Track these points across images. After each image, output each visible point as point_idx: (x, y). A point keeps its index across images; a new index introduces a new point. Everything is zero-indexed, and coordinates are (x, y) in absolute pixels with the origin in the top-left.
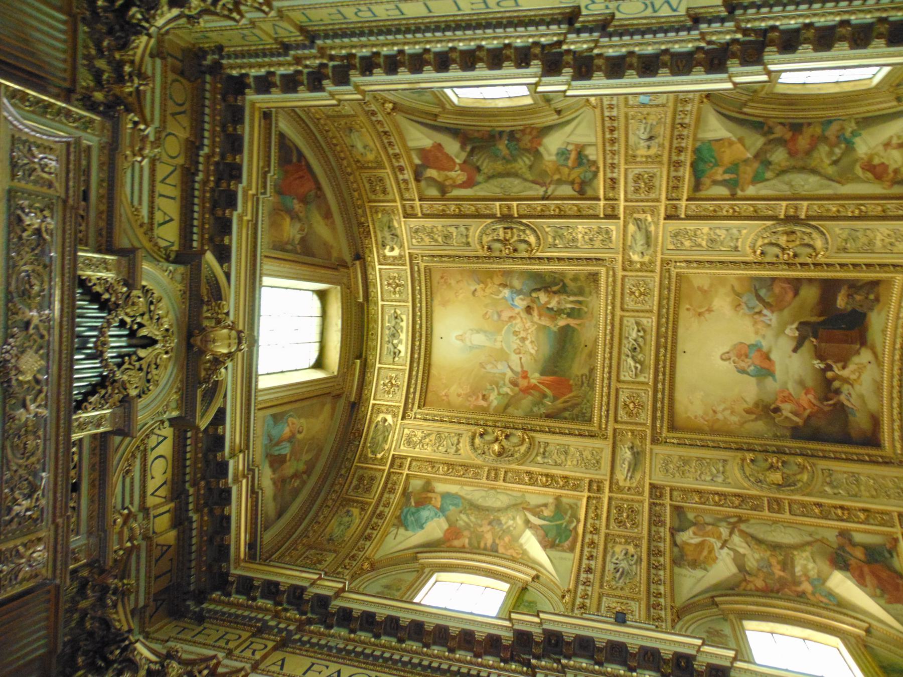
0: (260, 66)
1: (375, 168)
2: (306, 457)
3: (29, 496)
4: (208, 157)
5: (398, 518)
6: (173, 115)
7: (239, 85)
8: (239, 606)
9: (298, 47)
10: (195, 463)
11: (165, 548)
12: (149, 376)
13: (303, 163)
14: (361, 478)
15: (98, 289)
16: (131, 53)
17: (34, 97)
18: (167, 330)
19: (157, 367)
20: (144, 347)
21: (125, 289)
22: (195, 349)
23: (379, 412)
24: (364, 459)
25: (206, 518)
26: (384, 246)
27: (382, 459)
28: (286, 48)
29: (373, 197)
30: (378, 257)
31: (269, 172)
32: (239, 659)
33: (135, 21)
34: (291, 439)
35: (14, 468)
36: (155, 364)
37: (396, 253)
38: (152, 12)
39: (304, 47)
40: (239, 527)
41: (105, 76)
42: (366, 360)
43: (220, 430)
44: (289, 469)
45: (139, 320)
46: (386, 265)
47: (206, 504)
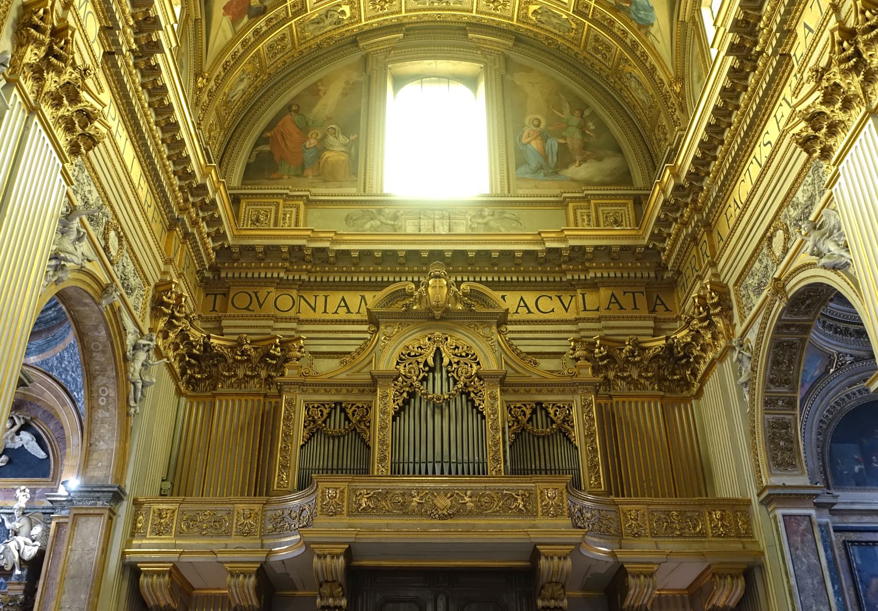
0: (204, 244)
1: (260, 58)
2: (566, 114)
3: (516, 499)
4: (287, 270)
5: (640, 27)
6: (261, 306)
7: (224, 252)
8: (673, 246)
10: (546, 272)
11: (613, 300)
12: (464, 354)
13: (269, 134)
14: (596, 50)
15: (400, 402)
17: (281, 444)
18: (429, 339)
19: (457, 347)
20: (442, 359)
22: (444, 315)
23: (526, 16)
24: (575, 41)
25: (594, 265)
26: (339, 21)
27: (577, 24)
28: (187, 235)
29: (289, 46)
30: (352, 24)
31: (287, 194)
32: (705, 272)
33: (202, 348)
34: (544, 137)
35: (498, 508)
36: (454, 349)
37: (346, 8)
38: (194, 343)
39: (184, 224)
41: (249, 373)
42: (469, 24)
43: (518, 255)
44: (574, 139)
45: (421, 366)
46: (360, 15)
47: (583, 264)
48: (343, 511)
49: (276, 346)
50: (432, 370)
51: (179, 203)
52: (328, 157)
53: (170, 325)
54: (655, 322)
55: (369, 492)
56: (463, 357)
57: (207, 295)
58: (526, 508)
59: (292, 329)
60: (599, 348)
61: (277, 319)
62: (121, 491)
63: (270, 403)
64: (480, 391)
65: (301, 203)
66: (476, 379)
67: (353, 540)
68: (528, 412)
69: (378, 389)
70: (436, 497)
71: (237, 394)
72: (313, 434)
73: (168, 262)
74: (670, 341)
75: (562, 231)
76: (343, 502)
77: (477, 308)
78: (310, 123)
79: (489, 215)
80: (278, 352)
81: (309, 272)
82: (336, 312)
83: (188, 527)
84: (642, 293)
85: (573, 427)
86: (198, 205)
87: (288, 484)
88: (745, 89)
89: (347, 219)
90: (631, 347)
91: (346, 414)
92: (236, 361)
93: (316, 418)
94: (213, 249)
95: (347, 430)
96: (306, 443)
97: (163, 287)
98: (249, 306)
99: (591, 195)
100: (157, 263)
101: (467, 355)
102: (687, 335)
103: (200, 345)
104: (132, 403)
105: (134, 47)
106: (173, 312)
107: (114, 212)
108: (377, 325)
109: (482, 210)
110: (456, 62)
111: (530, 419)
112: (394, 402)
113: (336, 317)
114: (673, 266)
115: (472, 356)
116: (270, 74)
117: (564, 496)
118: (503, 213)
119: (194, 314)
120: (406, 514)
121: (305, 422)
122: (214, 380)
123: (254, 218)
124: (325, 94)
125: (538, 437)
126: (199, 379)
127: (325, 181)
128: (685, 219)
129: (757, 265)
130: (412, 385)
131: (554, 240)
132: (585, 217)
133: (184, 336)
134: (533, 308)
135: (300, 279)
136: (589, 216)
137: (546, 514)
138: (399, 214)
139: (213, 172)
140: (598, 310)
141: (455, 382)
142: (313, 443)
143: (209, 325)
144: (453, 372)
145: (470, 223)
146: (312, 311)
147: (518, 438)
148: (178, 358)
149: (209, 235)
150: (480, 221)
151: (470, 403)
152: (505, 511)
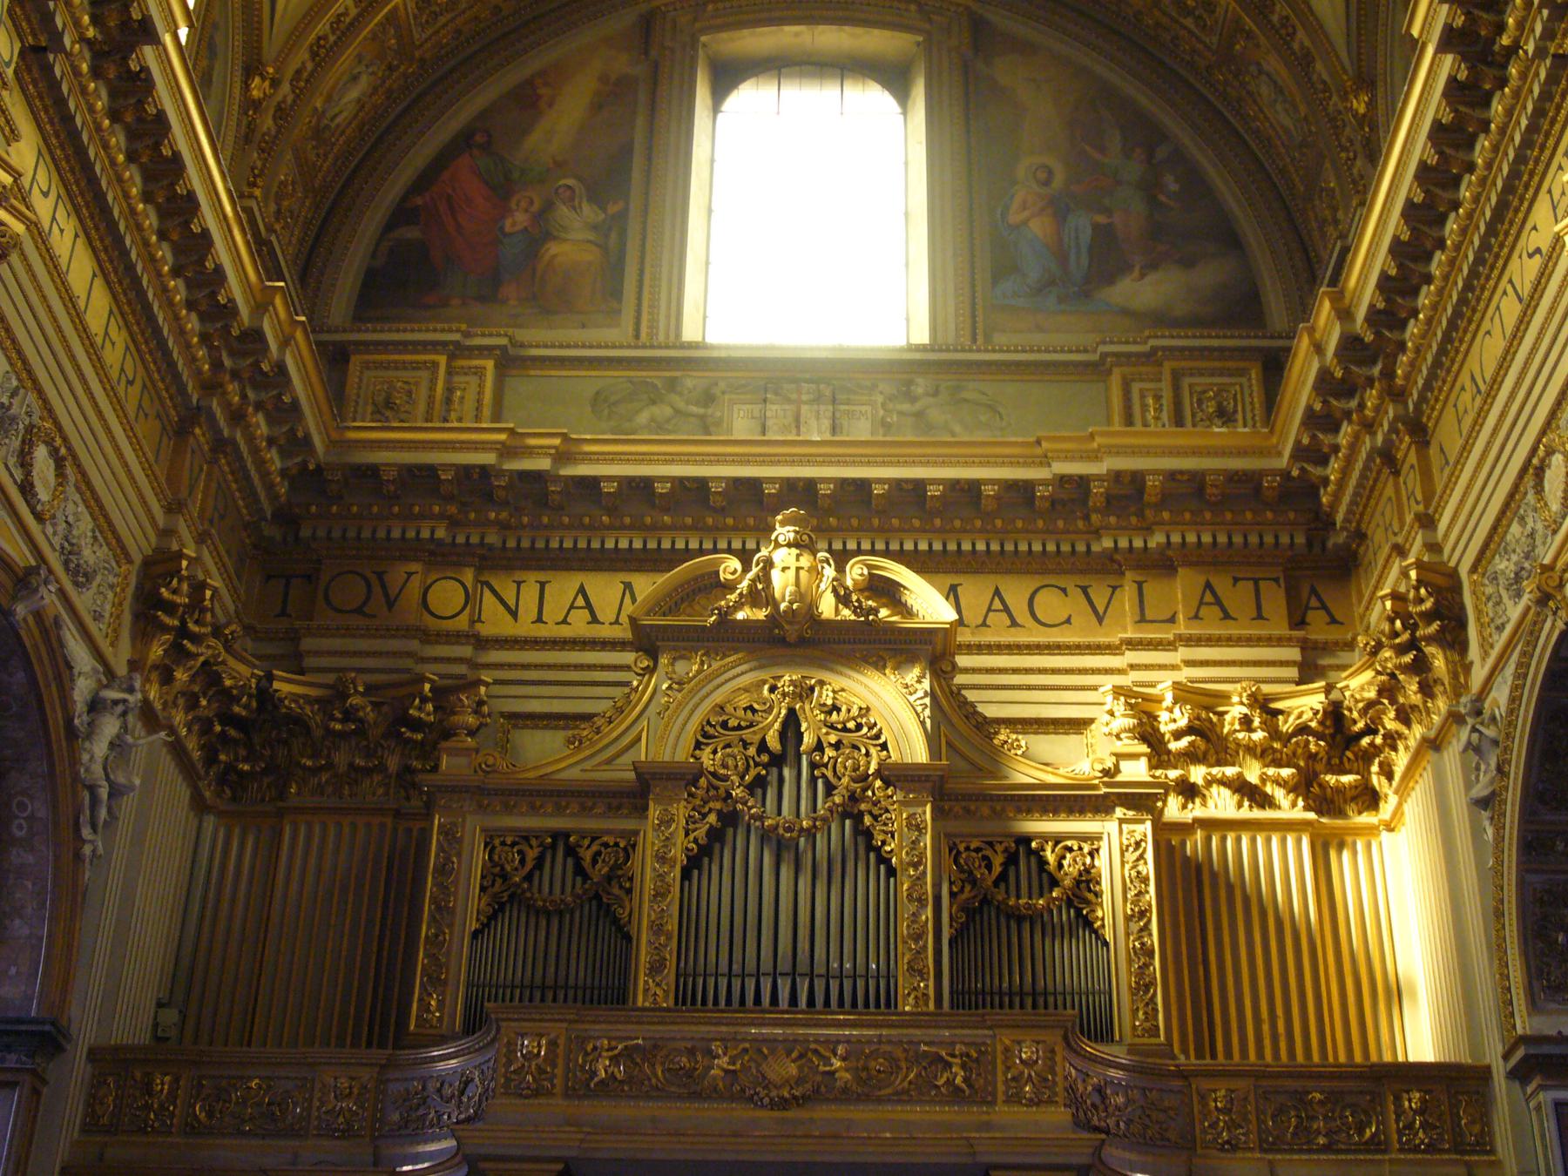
0: (261, 463)
3: (949, 1065)
8: (1345, 472)
11: (1209, 597)
12: (851, 725)
13: (419, 201)
15: (701, 833)
16: (308, 710)
17: (428, 929)
21: (703, 782)
33: (254, 704)
34: (1059, 208)
36: (830, 713)
38: (235, 692)
39: (212, 417)
41: (359, 762)
44: (1129, 214)
45: (752, 751)
48: (553, 1086)
49: (424, 700)
50: (777, 761)
51: (200, 372)
52: (554, 256)
53: (178, 653)
54: (1303, 649)
55: (613, 1043)
56: (850, 731)
57: (269, 577)
58: (970, 1086)
59: (460, 660)
61: (428, 637)
62: (59, 1031)
63: (409, 831)
64: (887, 811)
65: (490, 364)
66: (878, 783)
67: (573, 1153)
68: (998, 861)
69: (651, 804)
70: (765, 1057)
72: (502, 906)
74: (1335, 695)
75: (1092, 436)
76: (554, 1066)
78: (516, 175)
79: (927, 394)
80: (427, 713)
81: (504, 526)
82: (564, 622)
83: (210, 1115)
84: (1276, 580)
86: (246, 375)
87: (440, 1019)
88: (1485, 126)
89: (598, 400)
90: (1245, 710)
91: (578, 862)
92: (330, 732)
93: (508, 868)
94: (283, 473)
95: (579, 897)
96: (487, 925)
97: (160, 566)
98: (365, 603)
99: (1164, 349)
100: (149, 511)
101: (859, 727)
102: (1370, 683)
103: (250, 696)
104: (86, 833)
105: (91, 33)
106: (184, 623)
107: (45, 401)
108: (653, 655)
109: (910, 383)
110: (859, 30)
111: (1003, 877)
112: (687, 834)
113: (565, 632)
114: (1346, 520)
115: (870, 728)
116: (422, 60)
117: (1058, 1058)
119: (233, 627)
120: (696, 1096)
121: (483, 877)
123: (380, 399)
124: (550, 105)
126: (247, 773)
128: (1369, 413)
129: (1515, 528)
130: (729, 795)
131: (1069, 457)
132: (1150, 401)
133: (209, 675)
134: (1022, 615)
135: (482, 544)
136: (1158, 398)
137: (1014, 1098)
138: (717, 391)
139: (278, 301)
141: (830, 789)
143: (270, 650)
144: (826, 766)
145: (881, 412)
146: (509, 618)
147: (974, 920)
148: (196, 728)
149: (271, 441)
150: (906, 407)
151: (860, 839)
152: (922, 1091)
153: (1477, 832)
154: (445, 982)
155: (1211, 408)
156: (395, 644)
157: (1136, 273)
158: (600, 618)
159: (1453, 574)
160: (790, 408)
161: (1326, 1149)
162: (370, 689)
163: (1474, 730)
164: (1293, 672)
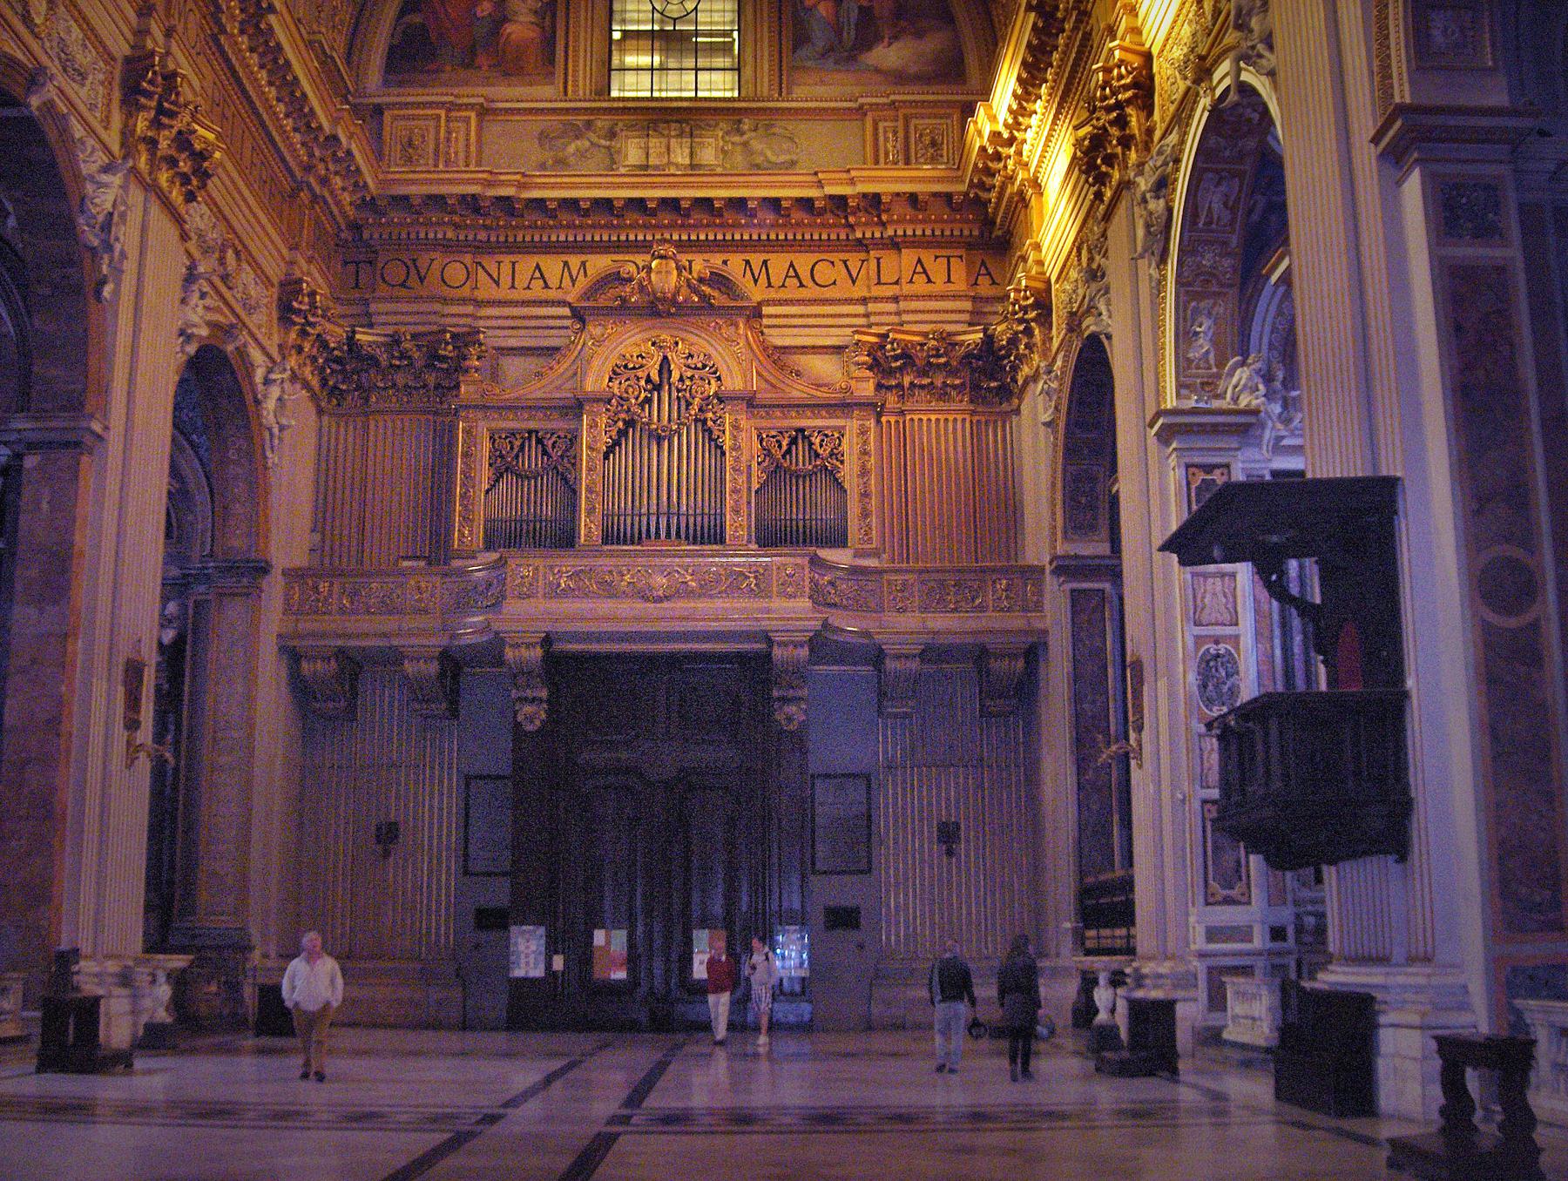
0: (338, 203)
4: (457, 226)
9: (311, 189)
12: (700, 365)
15: (614, 434)
18: (653, 344)
19: (691, 356)
36: (687, 358)
39: (309, 186)
40: (912, 180)
45: (643, 383)
49: (447, 344)
50: (658, 388)
52: (510, 34)
53: (303, 333)
57: (346, 263)
59: (467, 316)
60: (892, 343)
61: (445, 301)
65: (473, 115)
66: (715, 401)
68: (785, 443)
71: (399, 413)
72: (501, 475)
73: (293, 248)
77: (718, 298)
80: (448, 351)
82: (528, 288)
83: (352, 603)
84: (961, 257)
85: (842, 462)
92: (391, 366)
94: (351, 204)
101: (704, 366)
104: (269, 454)
108: (583, 321)
111: (789, 451)
113: (528, 295)
118: (769, 127)
122: (364, 391)
123: (405, 140)
125: (797, 477)
127: (507, 74)
130: (629, 410)
136: (895, 133)
138: (617, 129)
140: (897, 283)
142: (502, 485)
145: (721, 143)
150: (737, 139)
153: (1047, 438)
154: (472, 521)
155: (927, 140)
156: (425, 307)
157: (886, 43)
158: (551, 285)
159: (1048, 282)
160: (664, 141)
161: (953, 610)
162: (415, 336)
163: (1045, 383)
164: (966, 317)
